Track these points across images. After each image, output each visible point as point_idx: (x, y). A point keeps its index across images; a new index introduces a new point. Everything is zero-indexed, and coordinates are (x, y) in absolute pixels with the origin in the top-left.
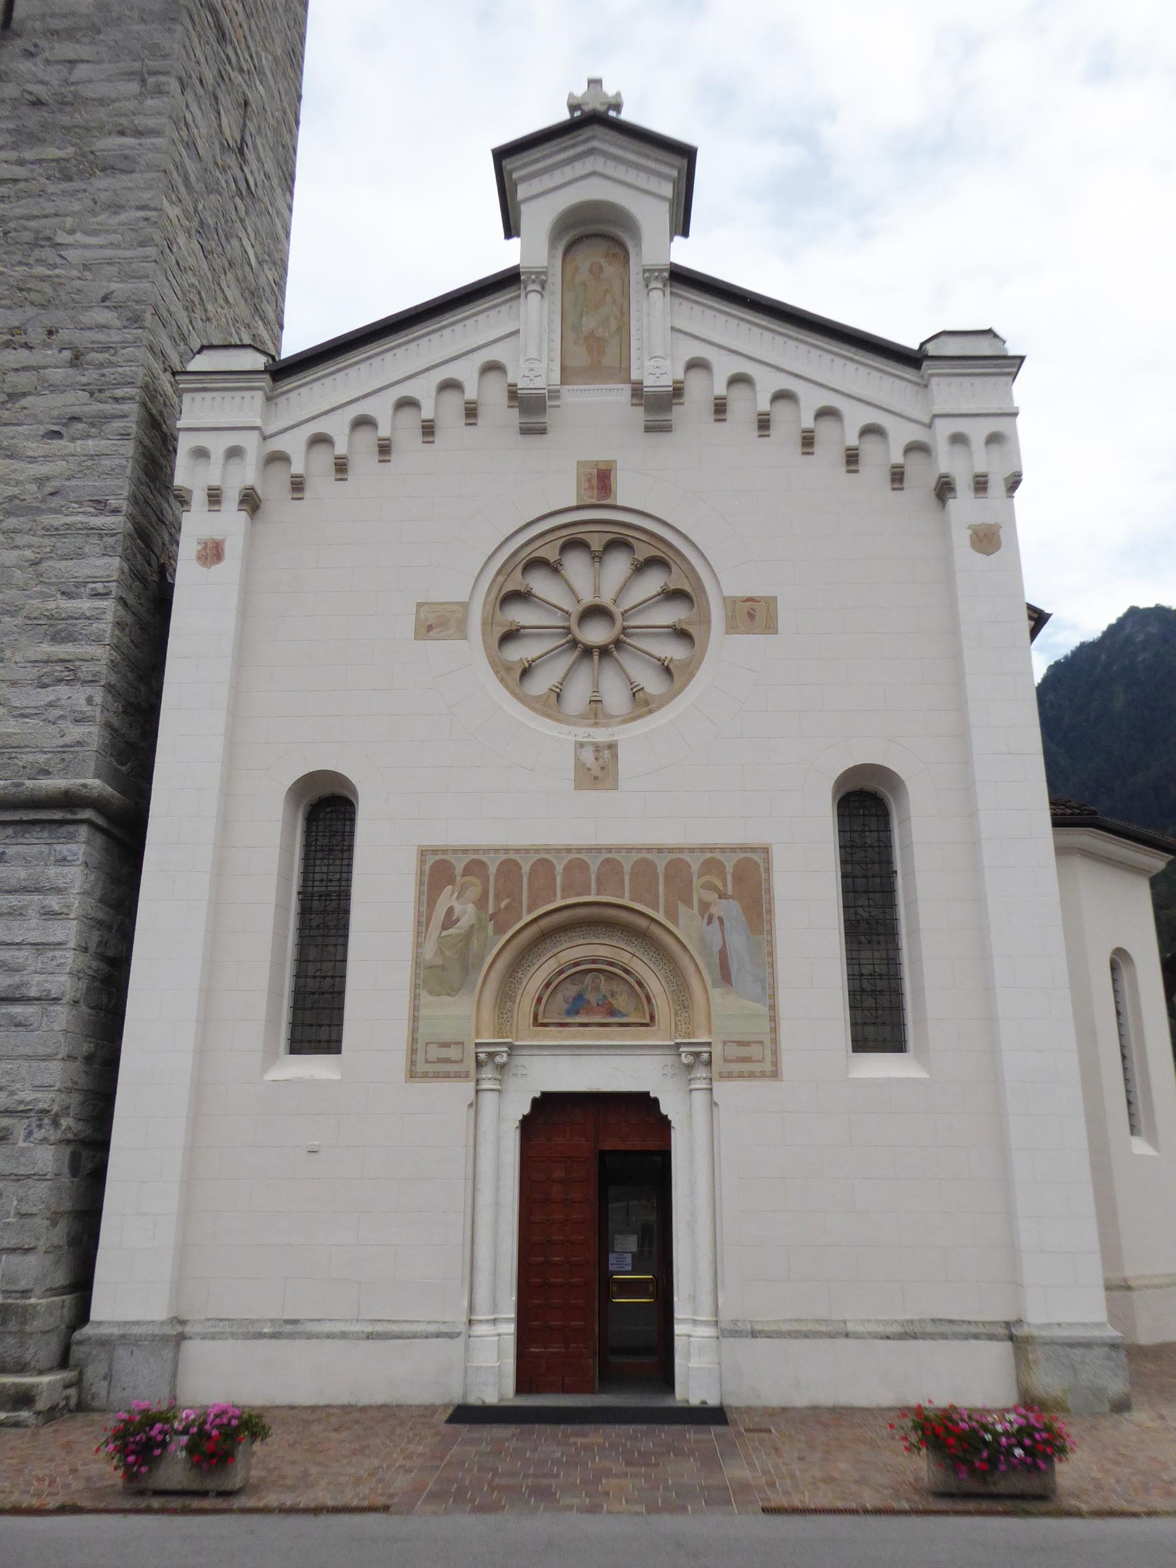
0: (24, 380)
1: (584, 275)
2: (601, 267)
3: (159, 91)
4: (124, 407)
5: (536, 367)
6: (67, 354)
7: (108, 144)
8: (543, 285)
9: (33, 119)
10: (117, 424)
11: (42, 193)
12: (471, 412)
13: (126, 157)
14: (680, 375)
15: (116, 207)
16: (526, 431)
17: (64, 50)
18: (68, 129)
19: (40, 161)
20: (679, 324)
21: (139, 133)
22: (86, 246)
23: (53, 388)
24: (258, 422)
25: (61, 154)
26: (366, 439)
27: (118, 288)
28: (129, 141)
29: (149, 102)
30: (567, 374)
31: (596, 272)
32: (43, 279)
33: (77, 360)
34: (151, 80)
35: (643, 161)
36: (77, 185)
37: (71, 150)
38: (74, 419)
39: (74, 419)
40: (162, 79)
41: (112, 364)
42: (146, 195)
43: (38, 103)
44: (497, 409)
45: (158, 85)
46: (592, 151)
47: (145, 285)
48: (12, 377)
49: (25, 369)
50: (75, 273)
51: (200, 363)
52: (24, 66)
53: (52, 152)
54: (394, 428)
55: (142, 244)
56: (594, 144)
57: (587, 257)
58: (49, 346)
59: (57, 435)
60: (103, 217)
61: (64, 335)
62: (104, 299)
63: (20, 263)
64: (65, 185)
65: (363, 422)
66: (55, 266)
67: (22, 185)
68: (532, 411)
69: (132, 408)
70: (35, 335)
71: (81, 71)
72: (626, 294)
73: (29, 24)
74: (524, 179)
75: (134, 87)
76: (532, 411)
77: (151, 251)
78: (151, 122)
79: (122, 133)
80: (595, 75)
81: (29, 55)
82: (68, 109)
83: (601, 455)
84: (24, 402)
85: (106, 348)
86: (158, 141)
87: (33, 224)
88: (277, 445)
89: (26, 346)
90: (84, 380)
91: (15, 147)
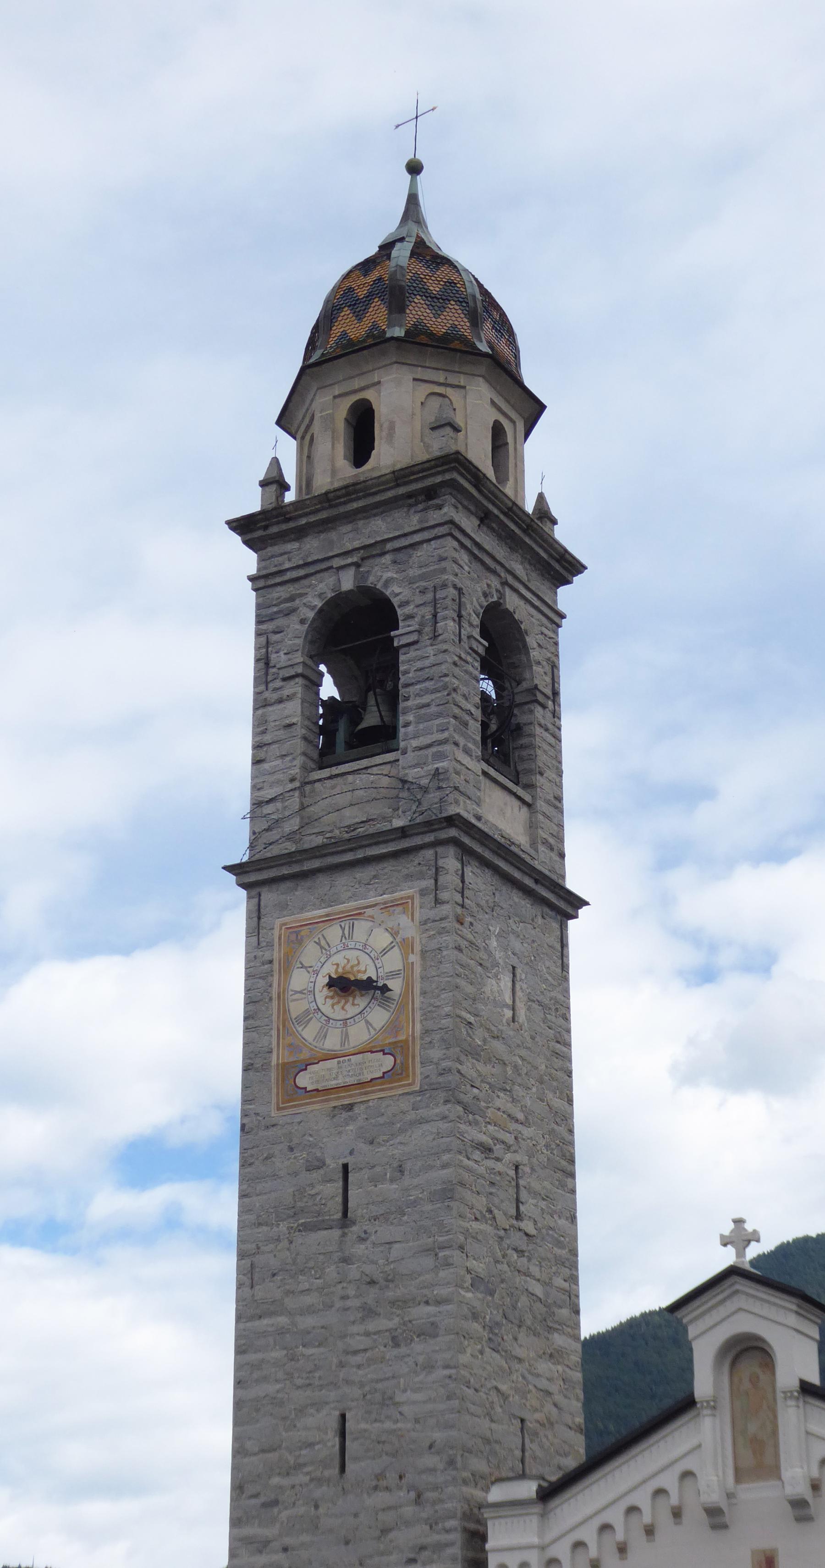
0: (388, 1518)
1: (746, 1385)
2: (758, 1377)
3: (447, 1264)
4: (452, 1537)
5: (713, 1481)
6: (413, 1495)
7: (421, 1313)
8: (714, 1408)
9: (372, 1295)
10: (450, 1551)
11: (383, 1360)
12: (677, 1513)
13: (432, 1324)
14: (815, 1473)
15: (429, 1367)
16: (715, 1527)
17: (385, 1232)
18: (393, 1303)
19: (378, 1332)
20: (814, 1428)
21: (438, 1303)
22: (414, 1403)
23: (408, 1524)
24: (535, 1540)
25: (390, 1324)
26: (610, 1542)
27: (438, 1436)
28: (431, 1309)
29: (442, 1274)
30: (740, 1475)
31: (754, 1381)
32: (392, 1432)
33: (418, 1500)
34: (441, 1254)
35: (772, 1299)
36: (403, 1350)
37: (397, 1320)
38: (423, 1548)
39: (423, 1548)
40: (447, 1252)
41: (441, 1501)
42: (448, 1355)
43: (372, 1282)
44: (694, 1514)
45: (446, 1258)
46: (737, 1292)
47: (454, 1433)
48: (381, 1516)
49: (390, 1508)
50: (409, 1426)
51: (496, 1494)
52: (360, 1249)
53: (384, 1323)
54: (627, 1530)
55: (449, 1398)
56: (738, 1287)
57: (749, 1366)
58: (400, 1488)
59: (412, 1561)
60: (421, 1377)
61: (409, 1478)
62: (431, 1447)
63: (376, 1421)
64: (395, 1352)
65: (606, 1528)
66: (397, 1421)
67: (368, 1354)
68: (716, 1518)
69: (457, 1537)
70: (392, 1478)
71: (396, 1251)
72: (775, 1400)
73: (359, 1212)
74: (691, 1321)
75: (428, 1262)
76: (716, 1518)
77: (455, 1403)
78: (444, 1292)
79: (427, 1303)
80: (737, 1216)
81: (362, 1240)
82: (391, 1285)
83: (765, 1544)
84: (392, 1535)
85: (436, 1488)
86: (449, 1307)
87: (379, 1386)
88: (553, 1552)
89: (387, 1489)
90: (424, 1515)
91: (363, 1319)
